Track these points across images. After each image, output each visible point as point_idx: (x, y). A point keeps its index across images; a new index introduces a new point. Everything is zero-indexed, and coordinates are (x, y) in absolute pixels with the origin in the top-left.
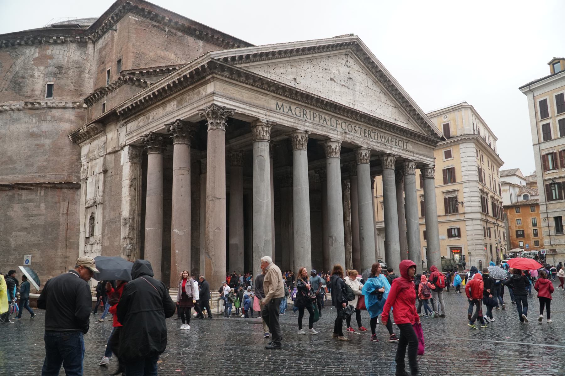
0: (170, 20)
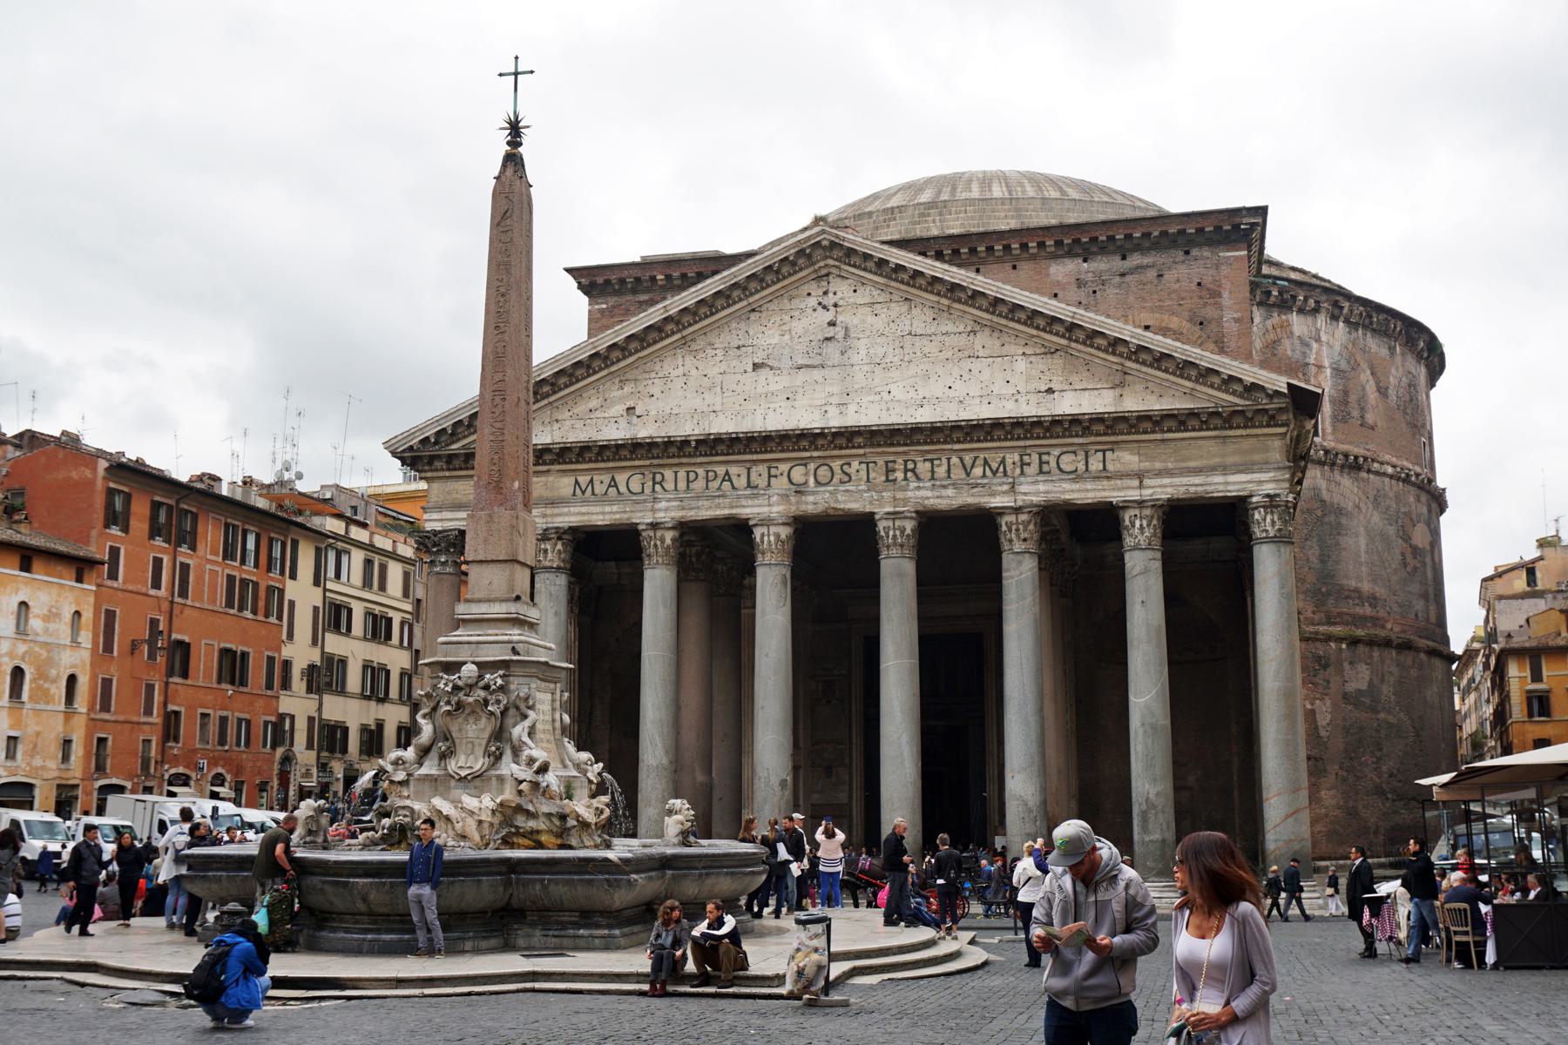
0: (668, 277)
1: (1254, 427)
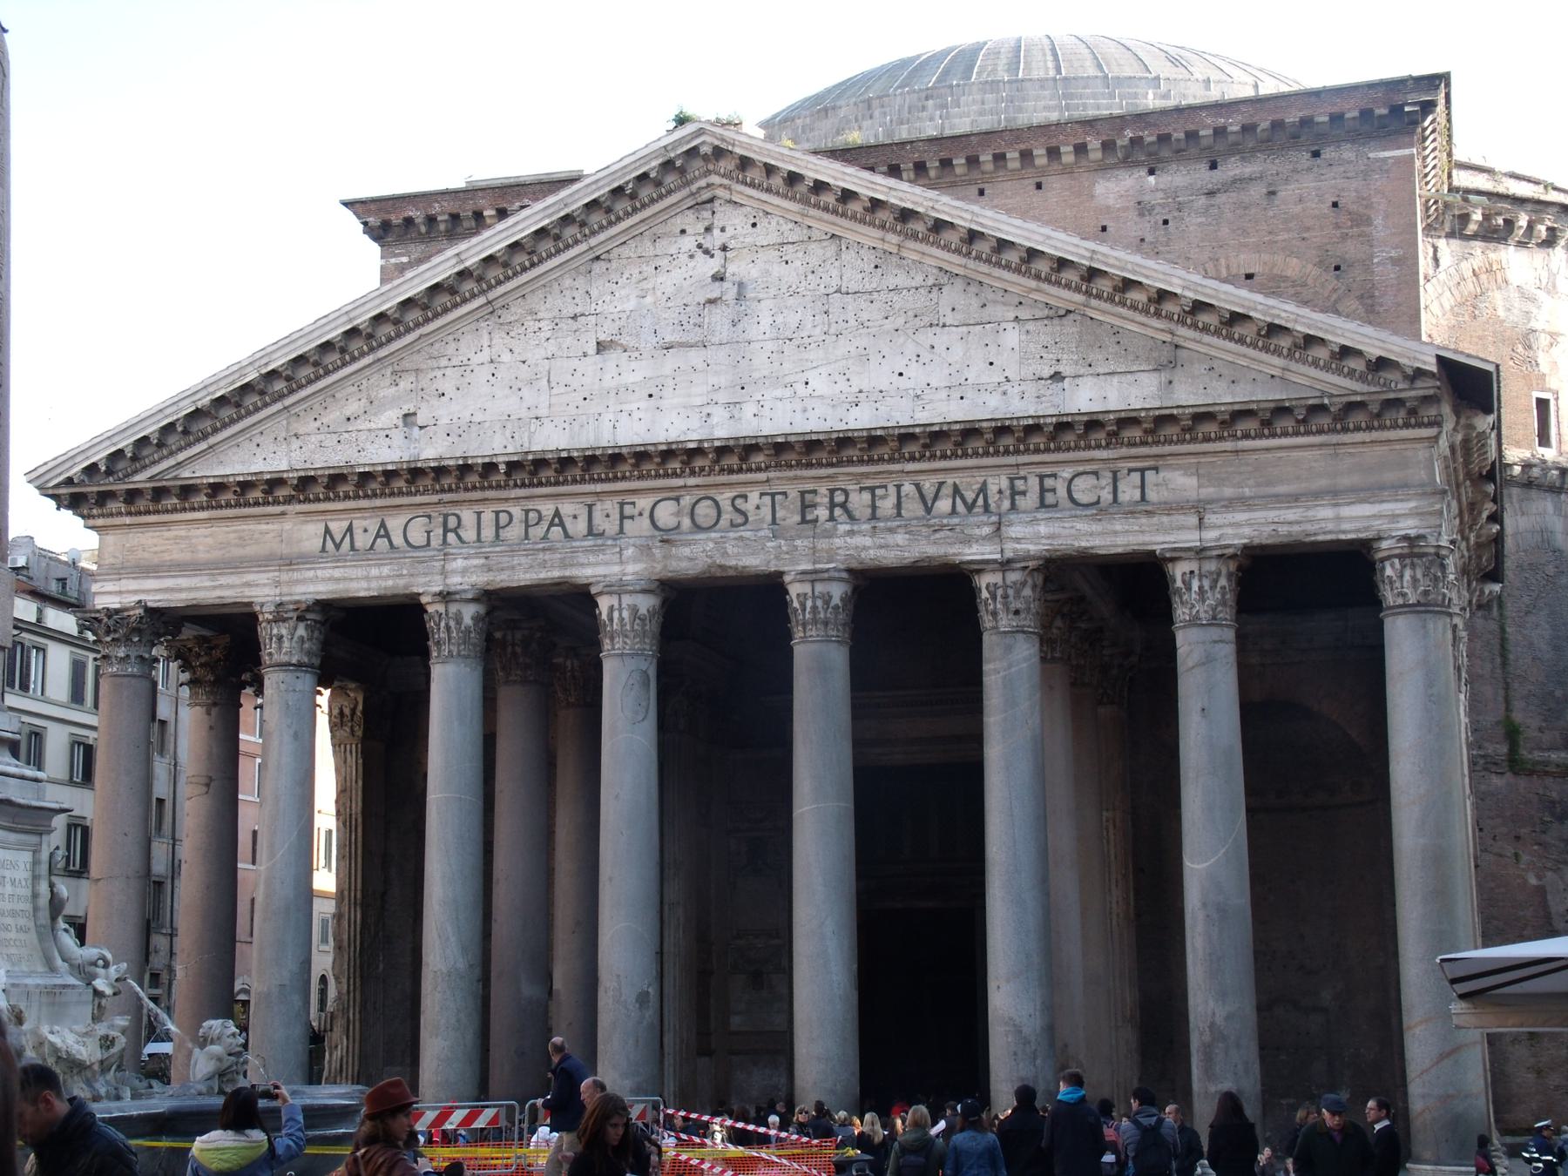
1: (1382, 427)
